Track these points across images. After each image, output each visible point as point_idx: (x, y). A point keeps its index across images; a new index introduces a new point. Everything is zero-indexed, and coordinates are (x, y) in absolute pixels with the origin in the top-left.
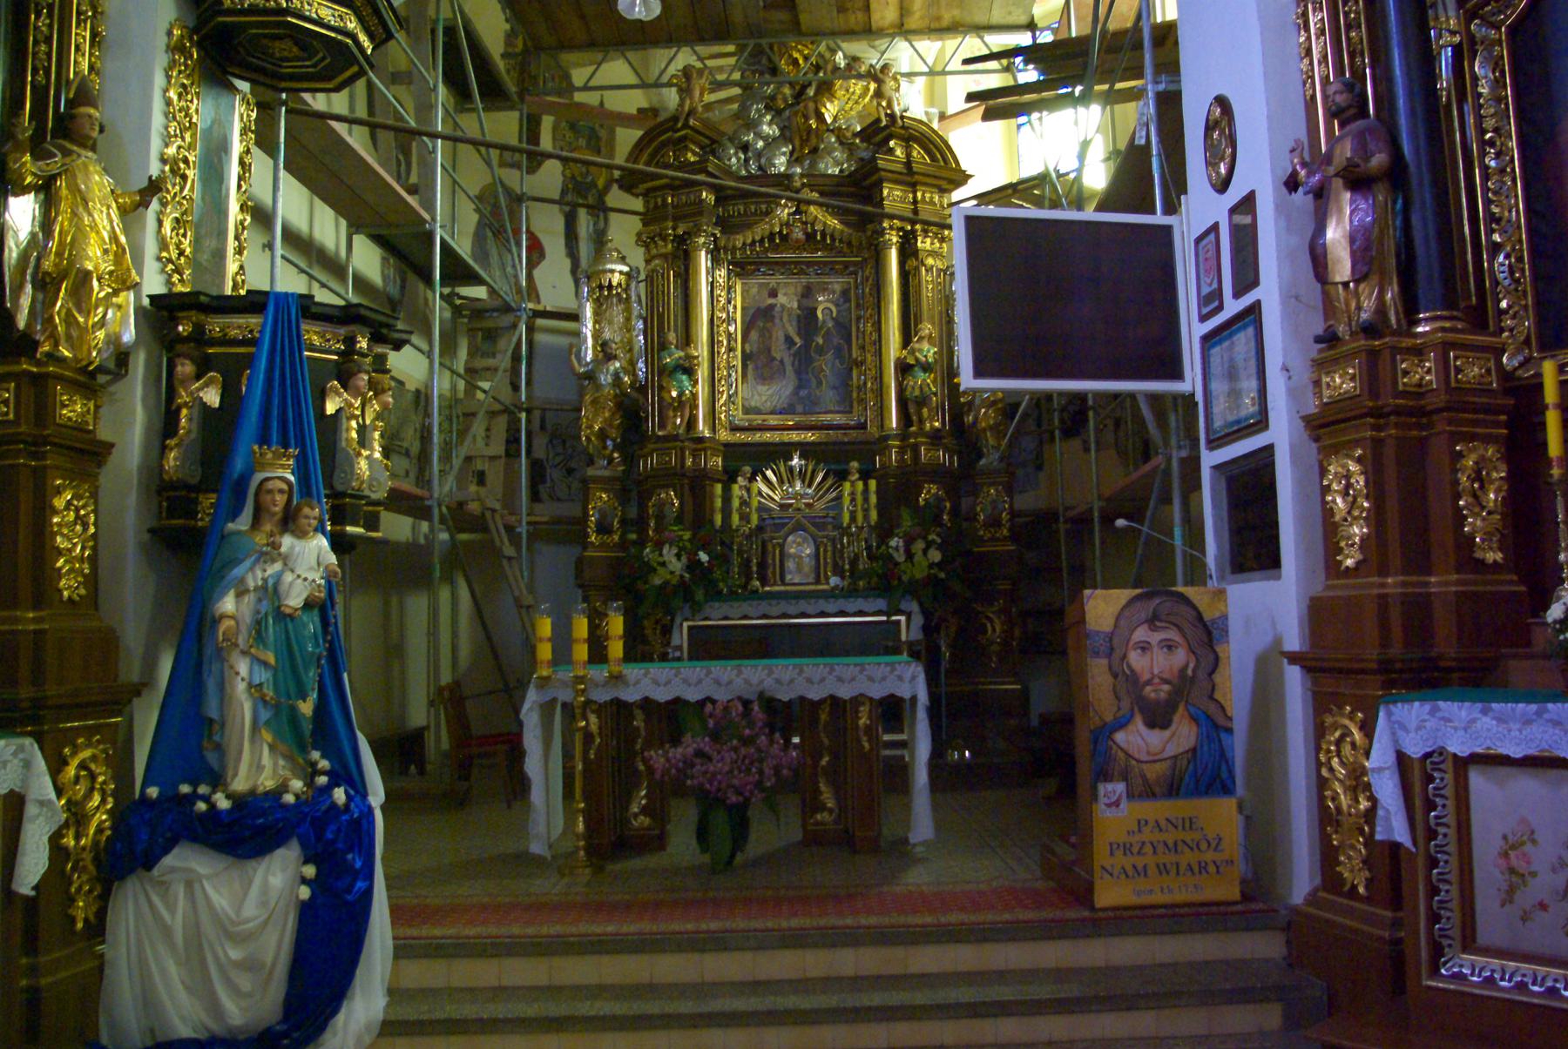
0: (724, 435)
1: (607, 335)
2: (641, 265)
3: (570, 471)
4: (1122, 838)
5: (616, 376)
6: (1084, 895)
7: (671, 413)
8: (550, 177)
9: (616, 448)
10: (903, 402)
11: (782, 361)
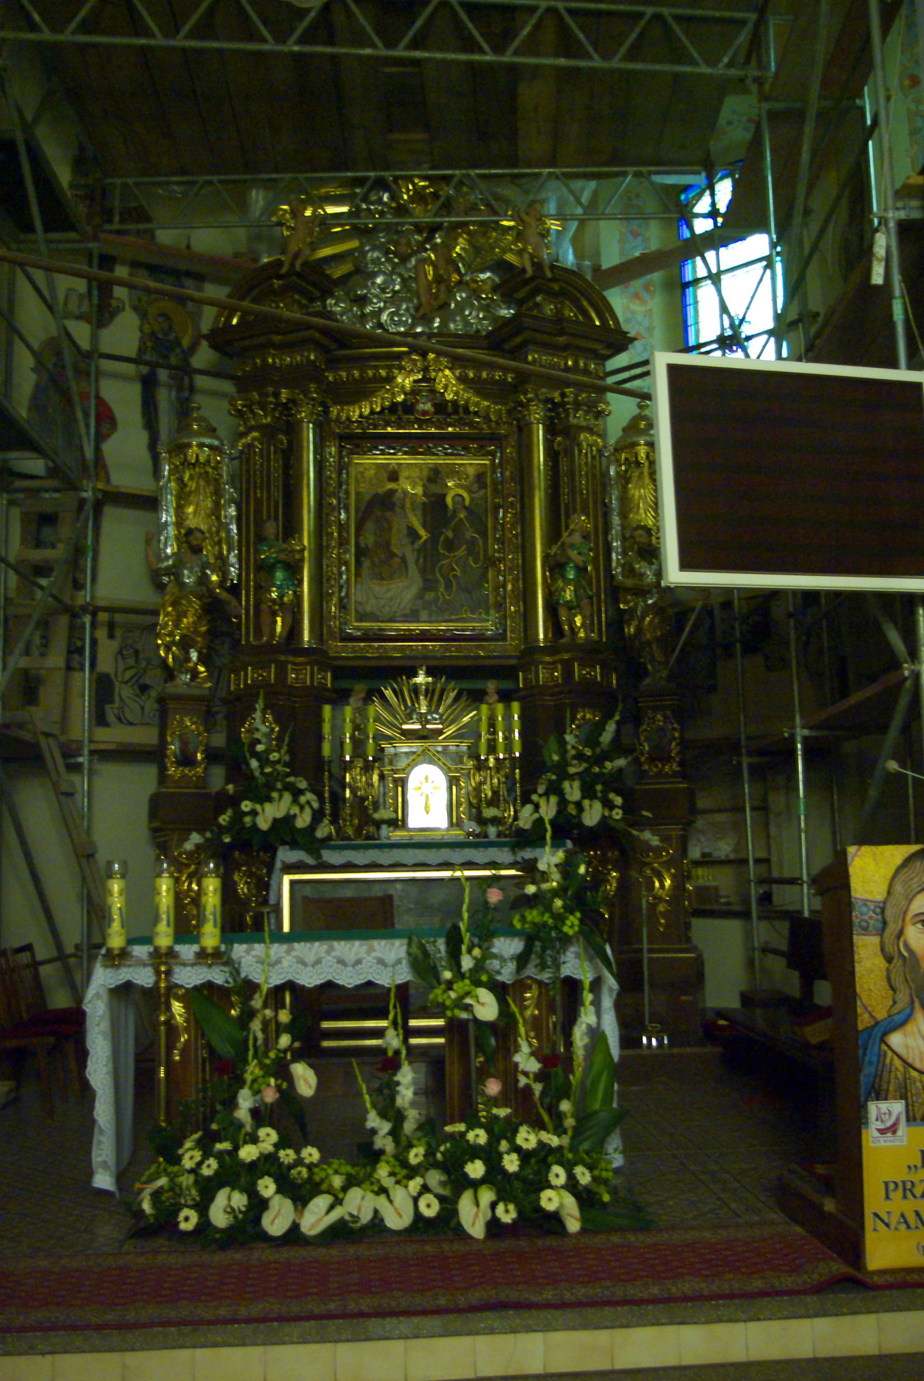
1: (191, 522)
3: (144, 688)
4: (902, 1175)
6: (853, 1249)
8: (124, 334)
9: (202, 660)
11: (404, 559)
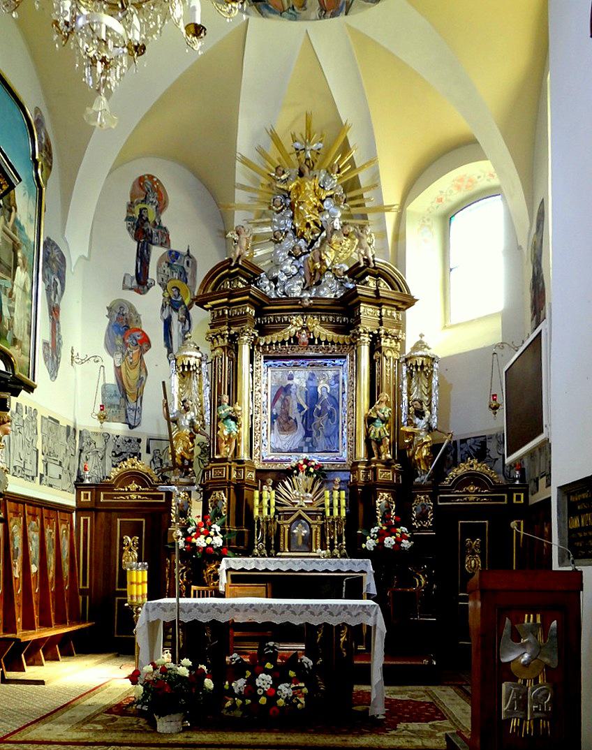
0: (258, 465)
2: (208, 353)
5: (192, 422)
7: (224, 445)
10: (368, 441)
11: (295, 421)
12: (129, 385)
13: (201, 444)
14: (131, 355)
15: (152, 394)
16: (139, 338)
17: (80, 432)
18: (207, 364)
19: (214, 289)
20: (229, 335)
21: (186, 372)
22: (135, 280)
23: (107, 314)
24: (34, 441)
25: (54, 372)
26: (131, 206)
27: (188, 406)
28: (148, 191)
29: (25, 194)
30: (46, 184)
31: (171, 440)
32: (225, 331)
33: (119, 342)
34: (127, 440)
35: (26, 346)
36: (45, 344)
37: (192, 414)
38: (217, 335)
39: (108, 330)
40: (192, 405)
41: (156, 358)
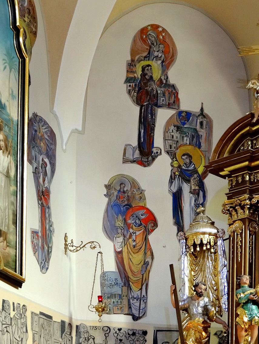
2: (226, 227)
5: (206, 311)
7: (244, 333)
12: (131, 271)
13: (218, 333)
14: (134, 237)
15: (158, 280)
16: (143, 217)
17: (77, 326)
18: (224, 240)
19: (232, 152)
20: (251, 204)
21: (198, 252)
22: (137, 152)
23: (105, 193)
24: (24, 340)
25: (44, 263)
26: (131, 65)
27: (200, 291)
28: (153, 45)
29: (5, 68)
30: (30, 53)
31: (180, 330)
32: (245, 200)
33: (119, 223)
34: (131, 333)
35: (11, 237)
36: (34, 233)
37: (206, 300)
38: (236, 206)
39: (107, 211)
40: (206, 290)
41: (165, 241)
